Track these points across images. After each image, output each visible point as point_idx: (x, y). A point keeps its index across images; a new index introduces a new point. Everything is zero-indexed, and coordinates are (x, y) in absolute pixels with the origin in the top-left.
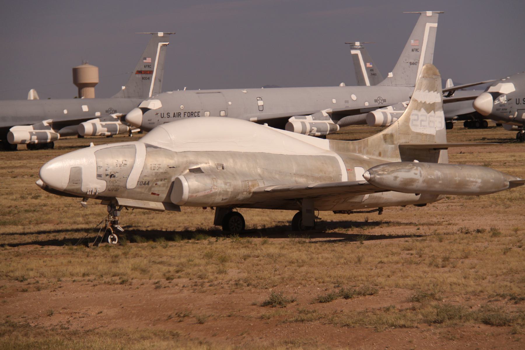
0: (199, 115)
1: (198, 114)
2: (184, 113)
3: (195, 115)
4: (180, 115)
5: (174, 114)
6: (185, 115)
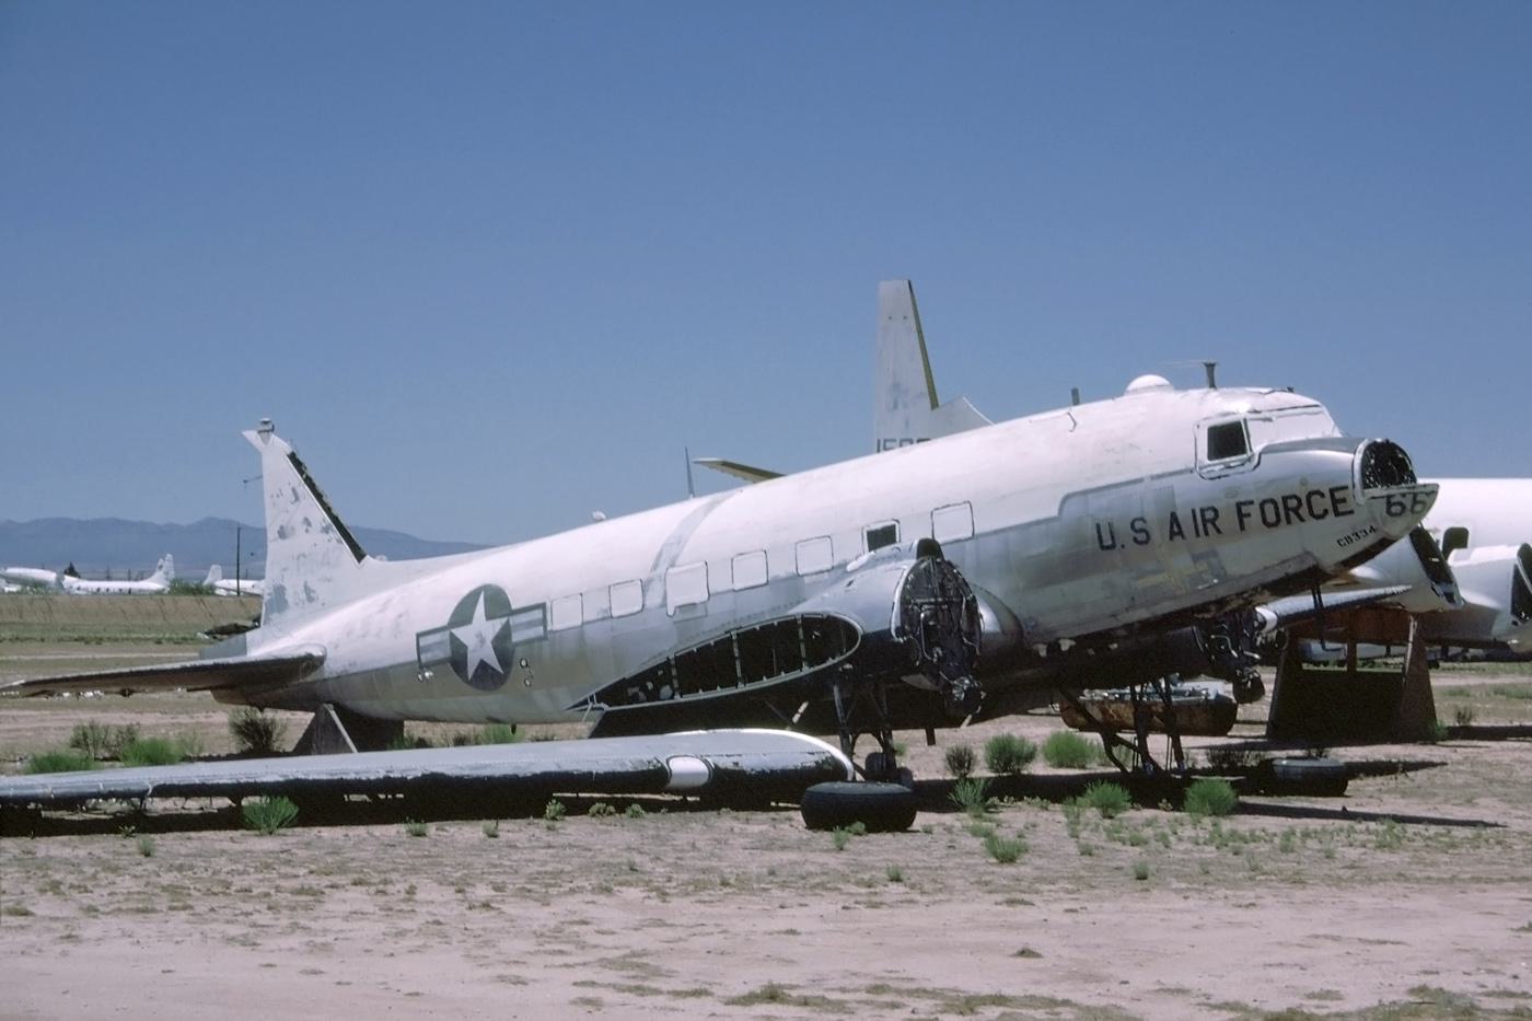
0: (1342, 508)
1: (1335, 502)
2: (1239, 505)
3: (1318, 510)
4: (1213, 522)
6: (1241, 516)
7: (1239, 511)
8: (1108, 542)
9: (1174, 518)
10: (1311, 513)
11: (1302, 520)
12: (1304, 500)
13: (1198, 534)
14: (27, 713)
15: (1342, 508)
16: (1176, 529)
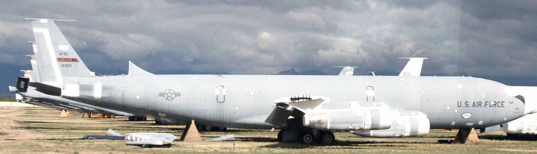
0: (503, 106)
1: (502, 104)
2: (486, 102)
3: (499, 106)
4: (480, 105)
5: (474, 103)
7: (486, 103)
8: (459, 105)
9: (474, 103)
10: (498, 106)
11: (496, 107)
12: (497, 103)
13: (477, 107)
14: (122, 113)
16: (474, 105)
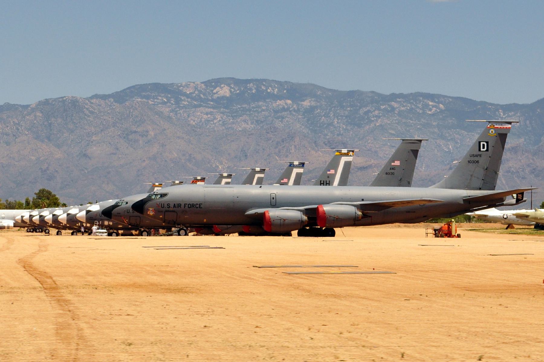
0: (200, 207)
1: (200, 206)
2: (185, 204)
3: (197, 207)
4: (180, 206)
5: (175, 204)
6: (185, 206)
9: (175, 204)
11: (194, 208)
12: (195, 205)
15: (200, 207)
